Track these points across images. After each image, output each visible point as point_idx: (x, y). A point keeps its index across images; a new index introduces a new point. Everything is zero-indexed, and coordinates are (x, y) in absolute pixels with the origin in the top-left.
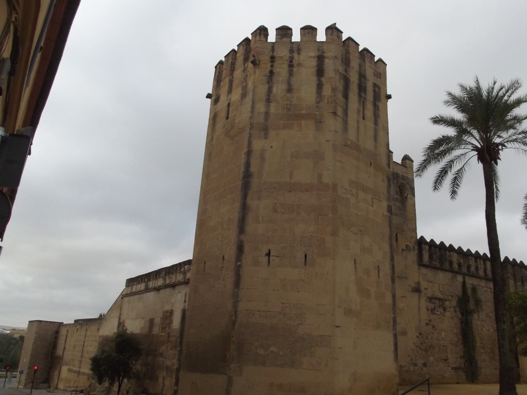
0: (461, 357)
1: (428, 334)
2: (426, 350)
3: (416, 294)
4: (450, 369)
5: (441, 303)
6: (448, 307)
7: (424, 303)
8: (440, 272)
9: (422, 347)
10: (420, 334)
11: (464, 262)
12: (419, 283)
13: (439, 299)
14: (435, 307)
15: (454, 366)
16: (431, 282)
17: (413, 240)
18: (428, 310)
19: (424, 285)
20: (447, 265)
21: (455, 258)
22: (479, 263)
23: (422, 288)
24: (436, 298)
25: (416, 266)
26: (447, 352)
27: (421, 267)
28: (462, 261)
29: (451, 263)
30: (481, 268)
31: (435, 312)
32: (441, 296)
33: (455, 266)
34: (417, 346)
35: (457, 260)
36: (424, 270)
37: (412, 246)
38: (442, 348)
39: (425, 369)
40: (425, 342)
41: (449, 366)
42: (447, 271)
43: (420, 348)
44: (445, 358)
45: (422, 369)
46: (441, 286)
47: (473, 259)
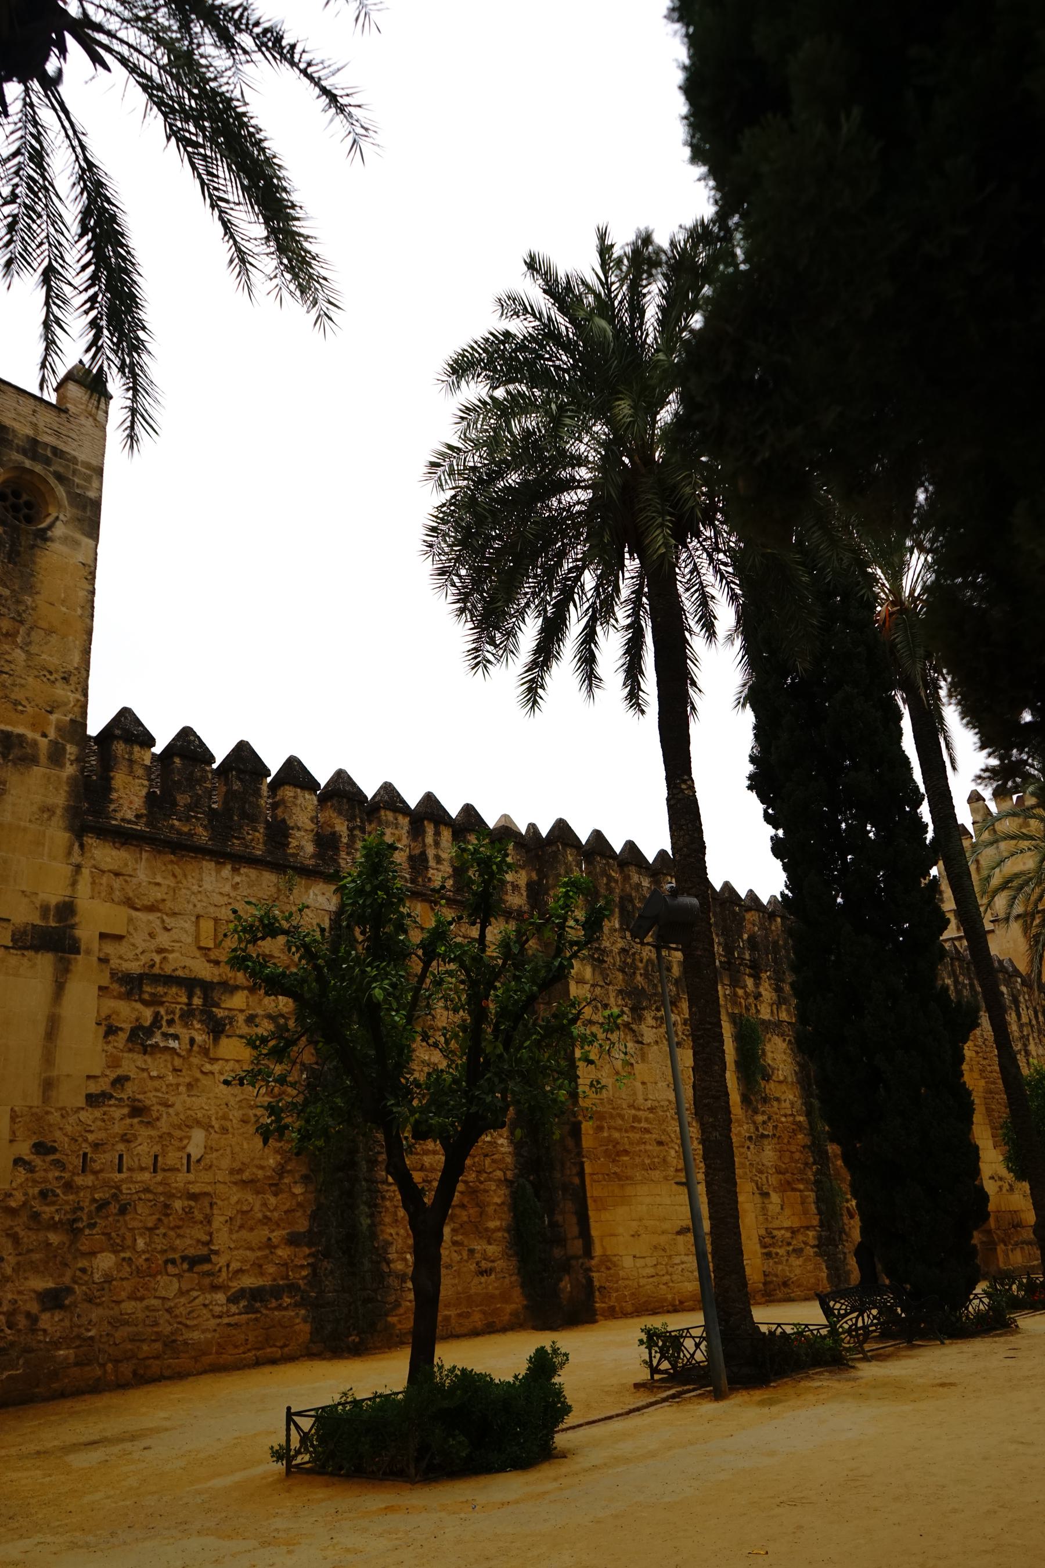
0: (293, 1240)
1: (96, 1146)
2: (72, 1228)
4: (221, 1297)
5: (197, 1001)
6: (241, 1018)
7: (84, 999)
8: (209, 866)
9: (48, 1211)
10: (41, 1148)
11: (351, 830)
12: (67, 910)
13: (190, 984)
15: (248, 1281)
16: (151, 909)
17: (53, 718)
18: (111, 1031)
19: (95, 915)
20: (256, 839)
21: (302, 812)
22: (429, 840)
23: (86, 933)
24: (170, 980)
25: (58, 835)
26: (208, 1220)
28: (341, 827)
29: (279, 833)
30: (438, 859)
31: (157, 1039)
33: (303, 845)
34: (12, 1212)
35: (314, 819)
37: (43, 742)
38: (178, 1204)
39: (50, 1322)
40: (69, 1186)
41: (215, 1288)
42: (253, 862)
43: (35, 1216)
45: (33, 1319)
46: (207, 926)
47: (404, 821)
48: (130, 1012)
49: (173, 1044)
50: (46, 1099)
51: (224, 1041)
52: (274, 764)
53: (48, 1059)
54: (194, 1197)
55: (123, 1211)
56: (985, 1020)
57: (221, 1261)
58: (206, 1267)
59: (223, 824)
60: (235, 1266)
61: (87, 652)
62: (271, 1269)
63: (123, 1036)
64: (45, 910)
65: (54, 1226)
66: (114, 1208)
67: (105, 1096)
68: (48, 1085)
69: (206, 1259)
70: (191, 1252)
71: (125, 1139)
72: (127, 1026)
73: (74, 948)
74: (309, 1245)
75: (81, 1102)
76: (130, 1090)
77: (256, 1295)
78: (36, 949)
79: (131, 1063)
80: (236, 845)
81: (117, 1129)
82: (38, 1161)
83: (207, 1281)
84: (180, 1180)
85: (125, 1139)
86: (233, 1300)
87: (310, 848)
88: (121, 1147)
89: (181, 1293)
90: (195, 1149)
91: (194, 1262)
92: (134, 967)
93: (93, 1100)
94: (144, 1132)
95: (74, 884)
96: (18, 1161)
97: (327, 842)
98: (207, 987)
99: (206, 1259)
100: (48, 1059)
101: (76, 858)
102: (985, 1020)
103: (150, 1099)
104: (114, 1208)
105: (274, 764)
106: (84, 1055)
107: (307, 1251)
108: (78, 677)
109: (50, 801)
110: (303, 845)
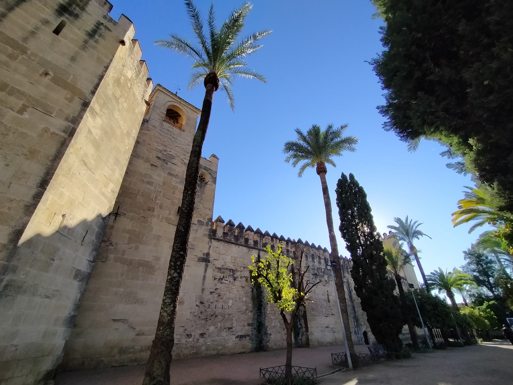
0: (249, 325)
2: (206, 319)
3: (203, 264)
4: (234, 337)
10: (202, 303)
12: (208, 254)
13: (230, 270)
14: (224, 277)
15: (240, 334)
24: (226, 269)
25: (207, 239)
26: (232, 320)
27: (213, 240)
31: (223, 281)
32: (232, 266)
36: (215, 243)
44: (231, 326)
47: (270, 238)
48: (219, 275)
49: (226, 282)
50: (203, 292)
51: (236, 281)
52: (246, 227)
53: (203, 284)
54: (229, 314)
55: (216, 316)
56: (397, 287)
57: (234, 329)
58: (231, 330)
59: (237, 238)
60: (237, 330)
61: (213, 205)
62: (244, 331)
63: (217, 280)
64: (204, 254)
65: (203, 319)
66: (214, 316)
67: (213, 292)
68: (203, 290)
69: (231, 328)
70: (229, 327)
71: (217, 301)
72: (218, 278)
73: (209, 262)
74: (252, 326)
75: (209, 293)
76: (218, 291)
77: (241, 337)
78: (202, 262)
79: (219, 286)
80: (239, 242)
81: (216, 299)
82: (201, 305)
83: (232, 333)
84: (227, 311)
85: (217, 301)
86: (237, 337)
87: (253, 243)
88: (216, 303)
89: (227, 336)
90: (230, 304)
91: (230, 328)
92: (220, 266)
93: (211, 293)
94: (221, 300)
95: (209, 249)
96: (197, 305)
97: (256, 242)
98: (233, 271)
99: (231, 328)
100: (203, 284)
101: (210, 244)
102: (397, 287)
103: (222, 293)
104: (214, 316)
105: (246, 227)
106: (210, 284)
107: (251, 327)
108: (211, 210)
109: (206, 233)
110: (251, 243)
